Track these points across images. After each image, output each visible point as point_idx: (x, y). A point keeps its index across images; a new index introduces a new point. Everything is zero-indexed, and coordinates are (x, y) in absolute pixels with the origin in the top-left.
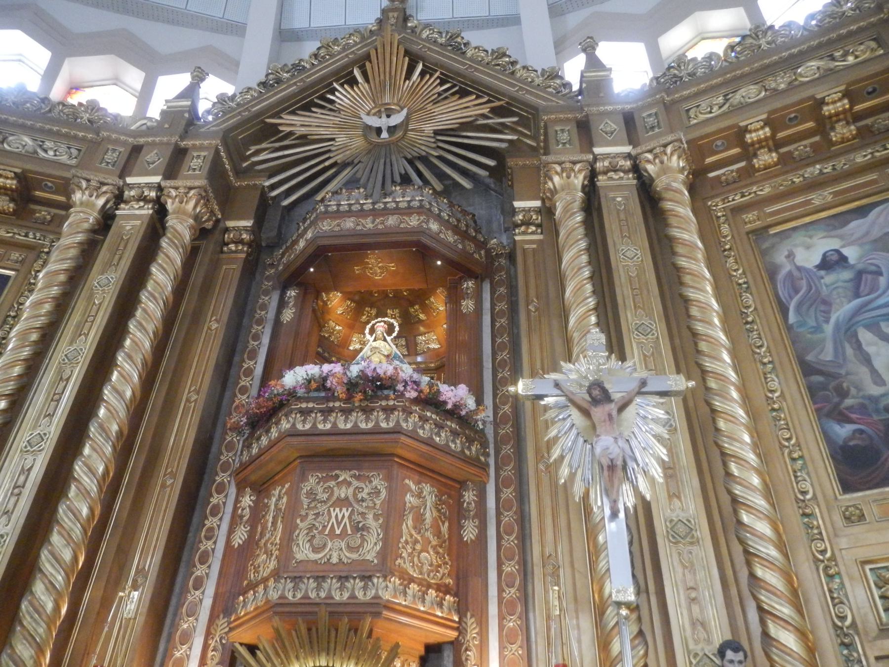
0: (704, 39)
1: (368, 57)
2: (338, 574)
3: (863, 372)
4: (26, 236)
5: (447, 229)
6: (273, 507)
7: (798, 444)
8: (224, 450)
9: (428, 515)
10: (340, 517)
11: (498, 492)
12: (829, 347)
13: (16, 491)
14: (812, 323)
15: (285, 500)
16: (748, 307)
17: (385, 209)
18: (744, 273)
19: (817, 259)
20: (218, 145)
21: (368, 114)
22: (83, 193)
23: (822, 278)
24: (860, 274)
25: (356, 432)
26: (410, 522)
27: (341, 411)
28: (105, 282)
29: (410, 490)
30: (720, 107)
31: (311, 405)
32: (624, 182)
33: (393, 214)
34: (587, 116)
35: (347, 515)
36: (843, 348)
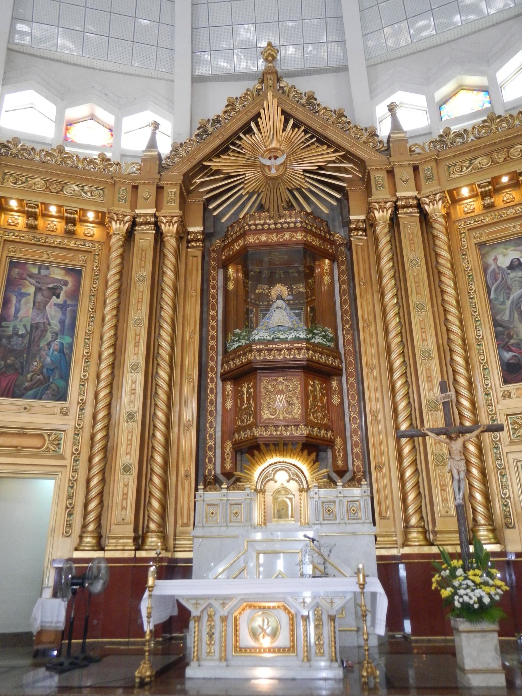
0: (462, 89)
1: (259, 115)
2: (284, 424)
4: (84, 245)
5: (316, 237)
6: (245, 392)
7: (487, 363)
8: (210, 361)
9: (318, 395)
10: (281, 399)
12: (508, 312)
13: (133, 392)
14: (501, 299)
15: (252, 390)
16: (472, 289)
17: (282, 228)
18: (471, 270)
19: (508, 264)
20: (181, 184)
21: (262, 157)
22: (116, 223)
23: (509, 274)
25: (285, 360)
26: (311, 399)
27: (276, 350)
28: (141, 278)
29: (310, 384)
30: (467, 168)
31: (261, 347)
33: (287, 232)
34: (392, 168)
35: (284, 398)
36: (514, 314)
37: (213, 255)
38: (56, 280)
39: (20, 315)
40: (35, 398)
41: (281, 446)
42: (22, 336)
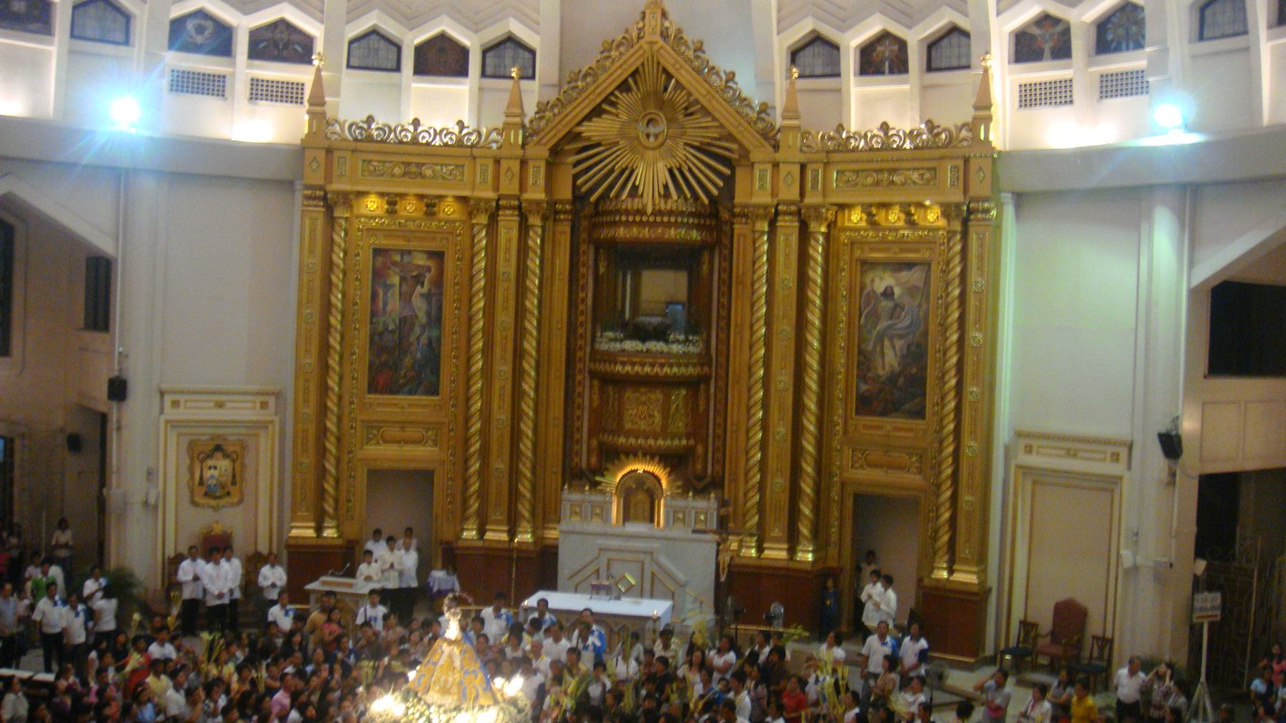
3: (879, 361)
11: (716, 382)
12: (872, 343)
23: (880, 302)
24: (896, 306)
32: (792, 224)
37: (585, 223)
38: (419, 267)
39: (389, 308)
40: (410, 393)
41: (640, 454)
42: (392, 331)
